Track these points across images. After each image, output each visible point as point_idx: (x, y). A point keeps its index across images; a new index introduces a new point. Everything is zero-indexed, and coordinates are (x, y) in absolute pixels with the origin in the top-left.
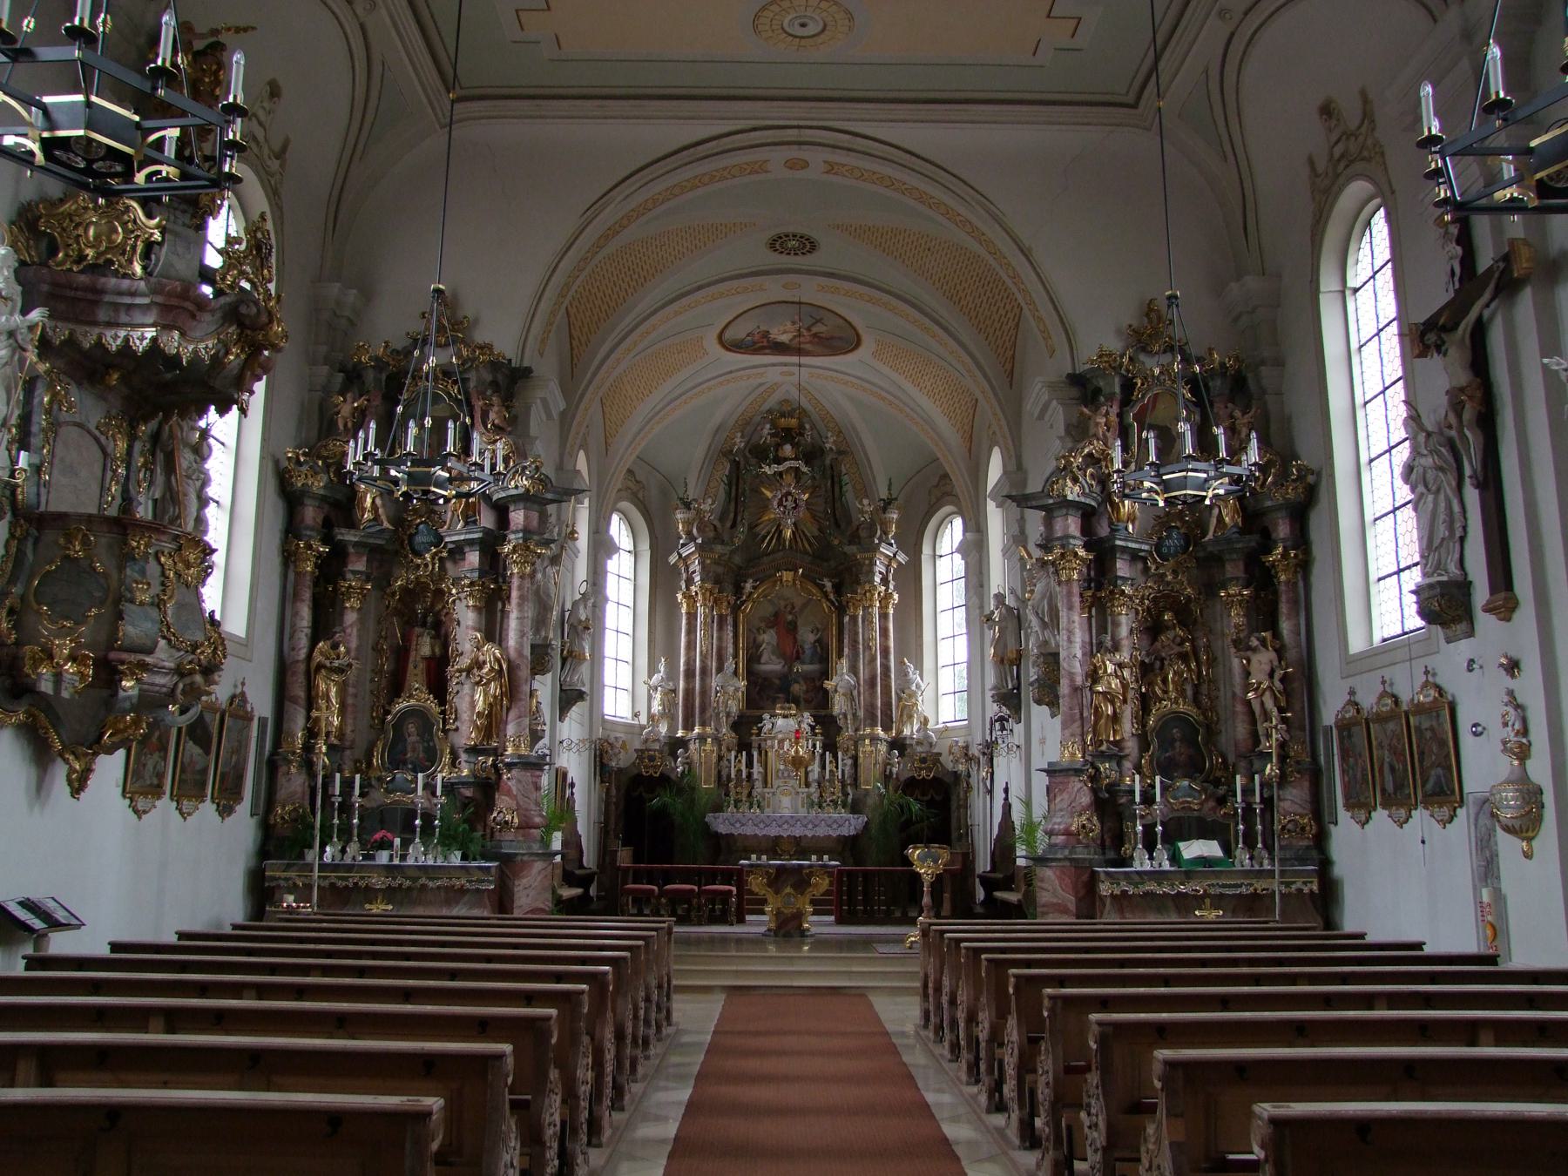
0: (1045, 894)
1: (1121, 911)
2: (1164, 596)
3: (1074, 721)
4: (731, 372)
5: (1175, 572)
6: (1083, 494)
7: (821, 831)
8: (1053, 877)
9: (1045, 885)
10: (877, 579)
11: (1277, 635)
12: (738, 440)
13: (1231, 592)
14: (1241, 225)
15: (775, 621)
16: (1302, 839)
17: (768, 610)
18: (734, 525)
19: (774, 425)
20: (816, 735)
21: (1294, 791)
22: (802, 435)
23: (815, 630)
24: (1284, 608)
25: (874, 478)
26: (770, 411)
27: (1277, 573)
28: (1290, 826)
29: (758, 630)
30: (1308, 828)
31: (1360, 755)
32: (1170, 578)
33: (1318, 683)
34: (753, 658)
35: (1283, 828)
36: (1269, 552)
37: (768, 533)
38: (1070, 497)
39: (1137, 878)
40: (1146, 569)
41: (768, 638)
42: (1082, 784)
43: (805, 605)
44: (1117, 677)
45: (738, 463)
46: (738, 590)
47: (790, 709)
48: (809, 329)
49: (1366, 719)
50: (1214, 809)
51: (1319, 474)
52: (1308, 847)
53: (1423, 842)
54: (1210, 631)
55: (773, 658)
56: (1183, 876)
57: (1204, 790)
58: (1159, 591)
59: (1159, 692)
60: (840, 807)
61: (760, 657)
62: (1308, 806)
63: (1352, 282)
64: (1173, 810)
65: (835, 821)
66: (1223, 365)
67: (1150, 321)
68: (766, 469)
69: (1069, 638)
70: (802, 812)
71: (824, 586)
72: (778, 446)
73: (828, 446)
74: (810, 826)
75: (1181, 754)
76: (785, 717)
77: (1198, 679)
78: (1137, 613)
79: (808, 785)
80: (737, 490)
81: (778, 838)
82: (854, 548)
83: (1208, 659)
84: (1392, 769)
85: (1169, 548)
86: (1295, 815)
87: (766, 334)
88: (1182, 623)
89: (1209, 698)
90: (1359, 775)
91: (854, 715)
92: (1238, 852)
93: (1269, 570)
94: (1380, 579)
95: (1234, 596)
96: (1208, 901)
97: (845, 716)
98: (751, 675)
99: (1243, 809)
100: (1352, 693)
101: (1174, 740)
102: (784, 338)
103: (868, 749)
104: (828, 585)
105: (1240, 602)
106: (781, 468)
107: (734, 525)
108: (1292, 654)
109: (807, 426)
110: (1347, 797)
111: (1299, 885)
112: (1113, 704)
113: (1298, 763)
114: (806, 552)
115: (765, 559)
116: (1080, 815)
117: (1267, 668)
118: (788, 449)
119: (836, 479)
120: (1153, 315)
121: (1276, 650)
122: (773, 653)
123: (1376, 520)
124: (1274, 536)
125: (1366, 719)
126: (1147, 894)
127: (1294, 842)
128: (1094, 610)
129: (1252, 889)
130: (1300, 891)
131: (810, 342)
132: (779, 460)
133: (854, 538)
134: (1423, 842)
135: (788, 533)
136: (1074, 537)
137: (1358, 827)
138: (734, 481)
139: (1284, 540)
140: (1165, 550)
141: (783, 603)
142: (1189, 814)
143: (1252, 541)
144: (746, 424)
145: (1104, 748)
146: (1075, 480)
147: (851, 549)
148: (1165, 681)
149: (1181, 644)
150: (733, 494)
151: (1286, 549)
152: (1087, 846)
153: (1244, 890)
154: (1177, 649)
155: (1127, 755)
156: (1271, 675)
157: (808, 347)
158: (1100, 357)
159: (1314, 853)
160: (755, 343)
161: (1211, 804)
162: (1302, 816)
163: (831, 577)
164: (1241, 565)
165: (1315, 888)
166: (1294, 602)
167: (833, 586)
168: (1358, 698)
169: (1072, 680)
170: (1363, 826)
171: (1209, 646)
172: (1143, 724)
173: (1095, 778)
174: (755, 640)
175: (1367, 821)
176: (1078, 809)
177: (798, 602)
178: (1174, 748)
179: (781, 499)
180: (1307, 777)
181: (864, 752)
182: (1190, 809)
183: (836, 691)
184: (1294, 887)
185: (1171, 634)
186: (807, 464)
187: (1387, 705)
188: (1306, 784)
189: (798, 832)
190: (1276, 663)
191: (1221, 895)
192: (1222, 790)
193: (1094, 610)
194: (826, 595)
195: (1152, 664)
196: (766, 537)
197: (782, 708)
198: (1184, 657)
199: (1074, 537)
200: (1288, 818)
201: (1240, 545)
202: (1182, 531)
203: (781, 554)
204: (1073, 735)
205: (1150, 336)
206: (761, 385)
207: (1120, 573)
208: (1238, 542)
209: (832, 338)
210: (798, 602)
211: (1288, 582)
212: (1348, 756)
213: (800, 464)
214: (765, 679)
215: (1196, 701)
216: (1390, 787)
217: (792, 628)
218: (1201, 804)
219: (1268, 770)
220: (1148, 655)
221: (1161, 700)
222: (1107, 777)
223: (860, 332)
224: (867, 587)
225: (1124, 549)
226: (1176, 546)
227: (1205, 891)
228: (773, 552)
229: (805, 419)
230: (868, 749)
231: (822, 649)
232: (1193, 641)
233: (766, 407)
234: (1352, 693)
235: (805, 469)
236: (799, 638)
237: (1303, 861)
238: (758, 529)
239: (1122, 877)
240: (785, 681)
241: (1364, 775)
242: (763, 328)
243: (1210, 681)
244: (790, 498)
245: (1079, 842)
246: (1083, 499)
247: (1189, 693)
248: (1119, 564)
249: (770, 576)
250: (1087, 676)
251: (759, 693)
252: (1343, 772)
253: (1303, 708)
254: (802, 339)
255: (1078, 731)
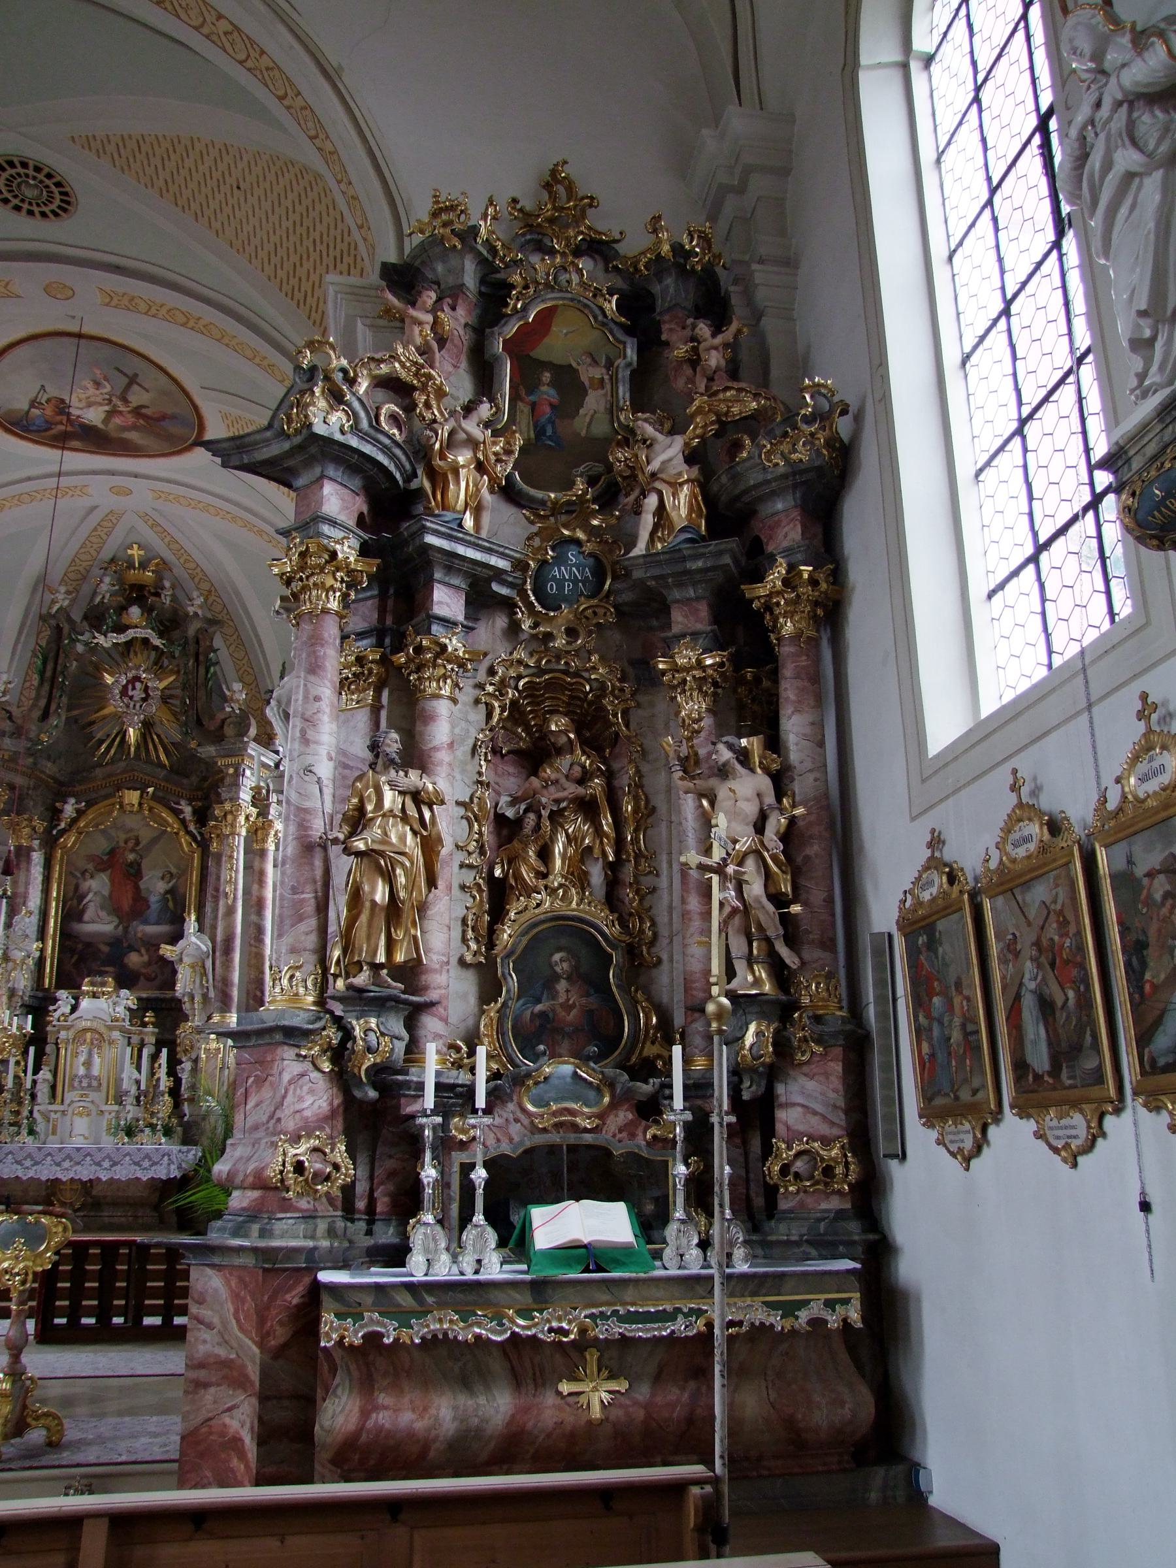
0: (206, 1335)
1: (367, 1385)
2: (549, 685)
3: (301, 919)
4: (29, 479)
5: (571, 633)
6: (356, 429)
7: (123, 1173)
8: (224, 1293)
9: (205, 1313)
10: (245, 796)
11: (774, 743)
12: (60, 597)
13: (681, 661)
14: (729, 70)
15: (109, 862)
16: (828, 1196)
17: (101, 845)
18: (45, 716)
19: (121, 580)
20: (144, 1025)
21: (811, 1085)
22: (158, 595)
23: (168, 876)
24: (789, 690)
25: (267, 665)
26: (113, 560)
27: (775, 620)
28: (799, 1166)
29: (83, 873)
30: (839, 1170)
31: (958, 985)
32: (560, 642)
33: (861, 848)
34: (72, 913)
35: (785, 1170)
36: (758, 576)
37: (108, 736)
38: (319, 429)
39: (405, 1300)
40: (514, 628)
41: (97, 886)
42: (307, 1065)
43: (155, 841)
44: (405, 818)
45: (59, 629)
46: (55, 814)
47: (103, 984)
48: (125, 400)
49: (974, 895)
50: (629, 1129)
51: (858, 419)
52: (840, 1215)
53: (1145, 1207)
54: (644, 754)
55: (103, 914)
56: (526, 1298)
57: (611, 1085)
58: (541, 672)
59: (527, 875)
60: (160, 1134)
61: (83, 912)
62: (840, 1118)
63: (922, 42)
64: (534, 1129)
65: (147, 1156)
66: (677, 248)
67: (553, 197)
68: (101, 640)
69: (303, 733)
70: (108, 1142)
71: (182, 812)
72: (122, 609)
73: (191, 610)
74: (106, 1164)
75: (568, 1007)
76: (95, 996)
77: (617, 853)
78: (489, 716)
79: (119, 1101)
80: (55, 669)
81: (56, 1181)
82: (208, 751)
83: (636, 810)
84: (1046, 1006)
85: (560, 583)
86: (812, 1138)
87: (62, 407)
88: (591, 744)
89: (637, 892)
90: (956, 1036)
91: (205, 996)
92: (671, 1231)
93: (759, 615)
94: (991, 595)
95: (687, 670)
96: (592, 1356)
97: (192, 998)
98: (66, 935)
99: (687, 1126)
100: (936, 841)
101: (556, 977)
102: (94, 416)
103: (214, 1045)
104: (187, 810)
105: (700, 681)
106: (122, 638)
107: (45, 716)
108: (802, 785)
109: (167, 584)
110: (928, 1094)
111: (816, 1309)
112: (390, 880)
113: (817, 1019)
114: (160, 765)
115: (98, 770)
116: (296, 1139)
117: (751, 809)
118: (135, 612)
119: (201, 658)
120: (561, 190)
121: (767, 771)
122: (102, 908)
123: (980, 471)
124: (770, 548)
125: (974, 895)
126: (432, 1343)
127: (809, 1200)
128: (385, 694)
129: (700, 1324)
130: (817, 1323)
131: (134, 427)
132: (121, 629)
133: (218, 737)
134: (1145, 1207)
135: (132, 734)
136: (333, 523)
137: (955, 1165)
138: (52, 655)
139: (788, 552)
140: (552, 588)
141: (123, 836)
142: (572, 1138)
143: (726, 552)
144: (78, 578)
145: (362, 979)
146: (336, 398)
147: (208, 751)
148: (545, 854)
149: (583, 780)
150: (48, 674)
151: (791, 568)
152: (310, 1217)
153: (679, 1326)
154: (573, 790)
155: (432, 1004)
156: (760, 828)
157: (133, 436)
158: (435, 214)
159: (854, 1228)
160: (49, 425)
161: (624, 1116)
162: (826, 1142)
163: (190, 801)
164: (704, 610)
165: (854, 1315)
166: (815, 678)
167: (195, 812)
168: (949, 854)
169: (303, 826)
170: (967, 1161)
171: (640, 786)
172: (491, 945)
173: (340, 1054)
174: (77, 887)
175: (978, 1149)
176: (290, 1125)
177: (146, 836)
178: (554, 995)
179: (125, 687)
180: (838, 1051)
181: (207, 1051)
182: (575, 1127)
183: (181, 960)
184: (804, 1315)
185: (564, 762)
186: (161, 635)
187: (1027, 839)
188: (837, 1068)
189: (85, 1173)
190: (770, 799)
191: (625, 1341)
192: (646, 1088)
193: (385, 694)
194: (183, 822)
195: (519, 822)
196: (101, 742)
197: (92, 984)
198: (588, 808)
199: (333, 523)
200: (796, 1148)
201: (700, 564)
202: (588, 548)
203: (122, 765)
204: (293, 950)
205: (551, 221)
206: (93, 508)
207: (438, 610)
208: (696, 557)
209: (164, 417)
210: (146, 836)
211: (797, 636)
212: (931, 994)
213: (149, 633)
214: (88, 945)
215: (612, 900)
216: (1039, 1058)
217: (134, 873)
218: (601, 1116)
219: (749, 1038)
220: (514, 801)
221: (529, 891)
222: (369, 1050)
223: (199, 401)
224: (227, 806)
225: (452, 561)
226: (575, 581)
227: (583, 1331)
228: (113, 761)
229: (167, 574)
230: (214, 1045)
231: (175, 904)
232: (610, 777)
233: (106, 554)
234: (936, 841)
235: (157, 642)
236: (142, 885)
237: (828, 1247)
238: (95, 727)
239: (368, 1300)
240: (118, 948)
241: (969, 1035)
242: (53, 391)
243: (638, 856)
244: (138, 685)
245: (286, 1206)
246: (354, 442)
247: (597, 875)
248: (440, 594)
249: (106, 797)
250: (346, 818)
251: (76, 965)
252: (919, 1033)
253: (830, 901)
254: (117, 420)
255: (311, 941)
